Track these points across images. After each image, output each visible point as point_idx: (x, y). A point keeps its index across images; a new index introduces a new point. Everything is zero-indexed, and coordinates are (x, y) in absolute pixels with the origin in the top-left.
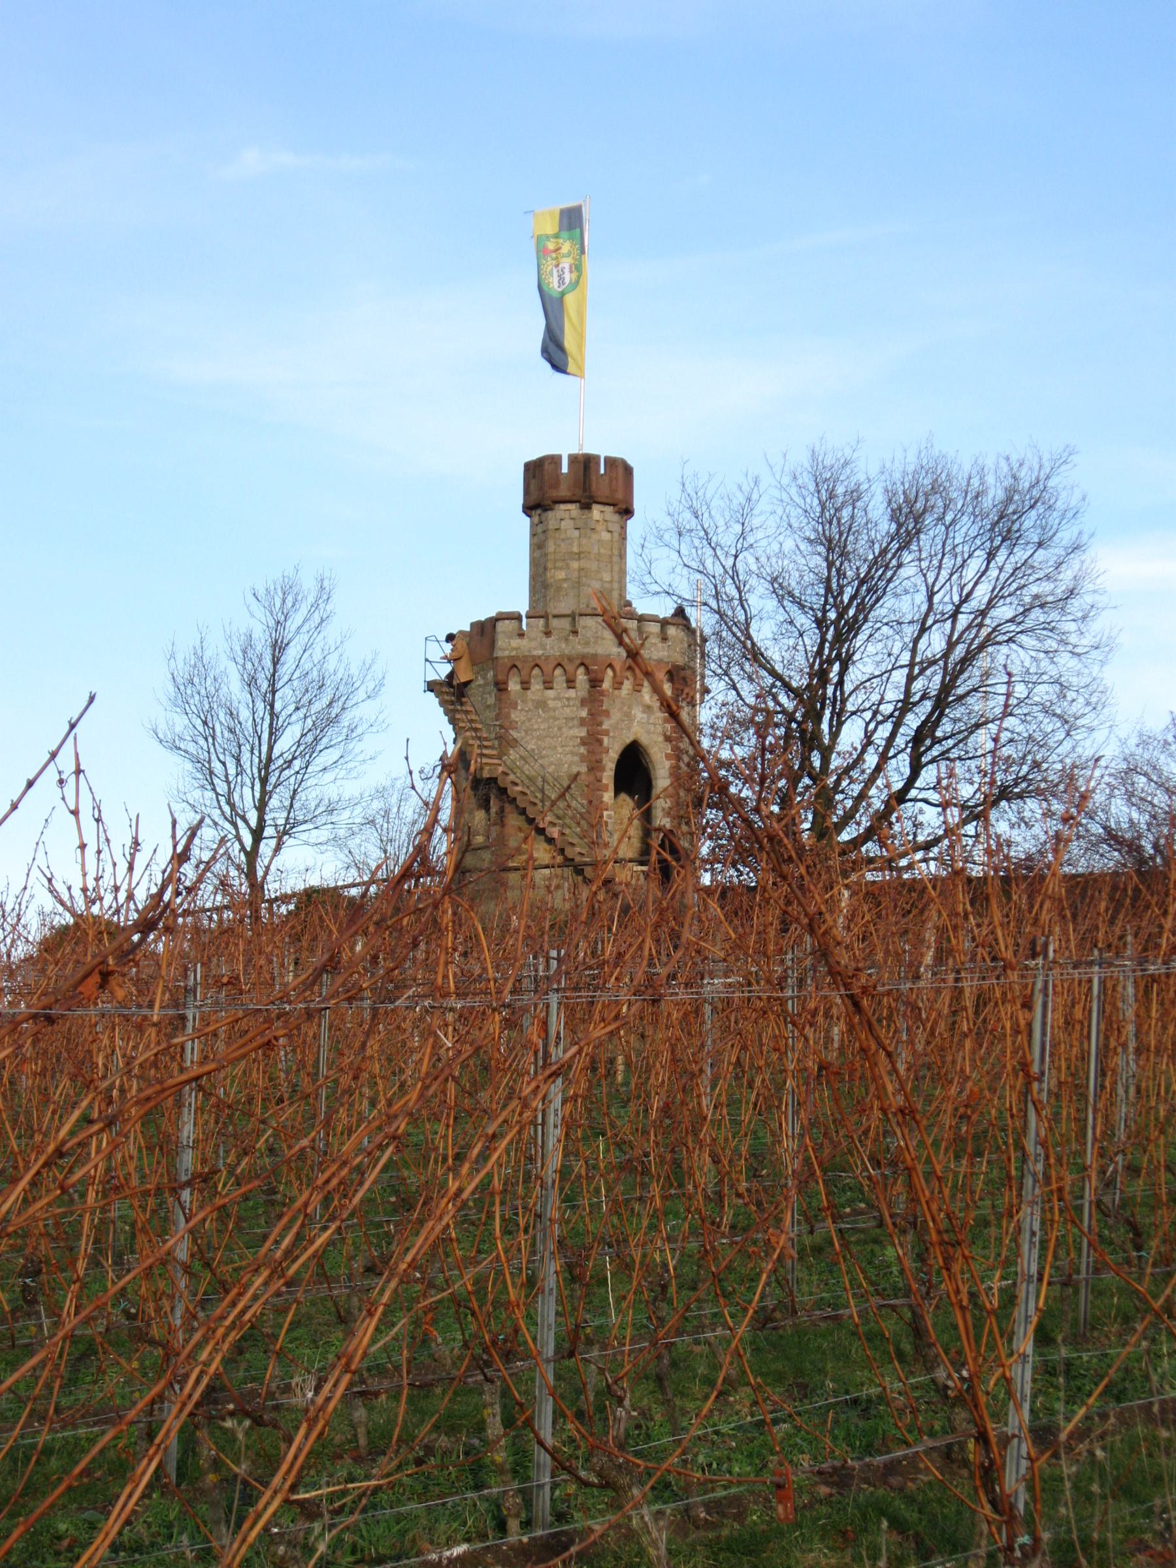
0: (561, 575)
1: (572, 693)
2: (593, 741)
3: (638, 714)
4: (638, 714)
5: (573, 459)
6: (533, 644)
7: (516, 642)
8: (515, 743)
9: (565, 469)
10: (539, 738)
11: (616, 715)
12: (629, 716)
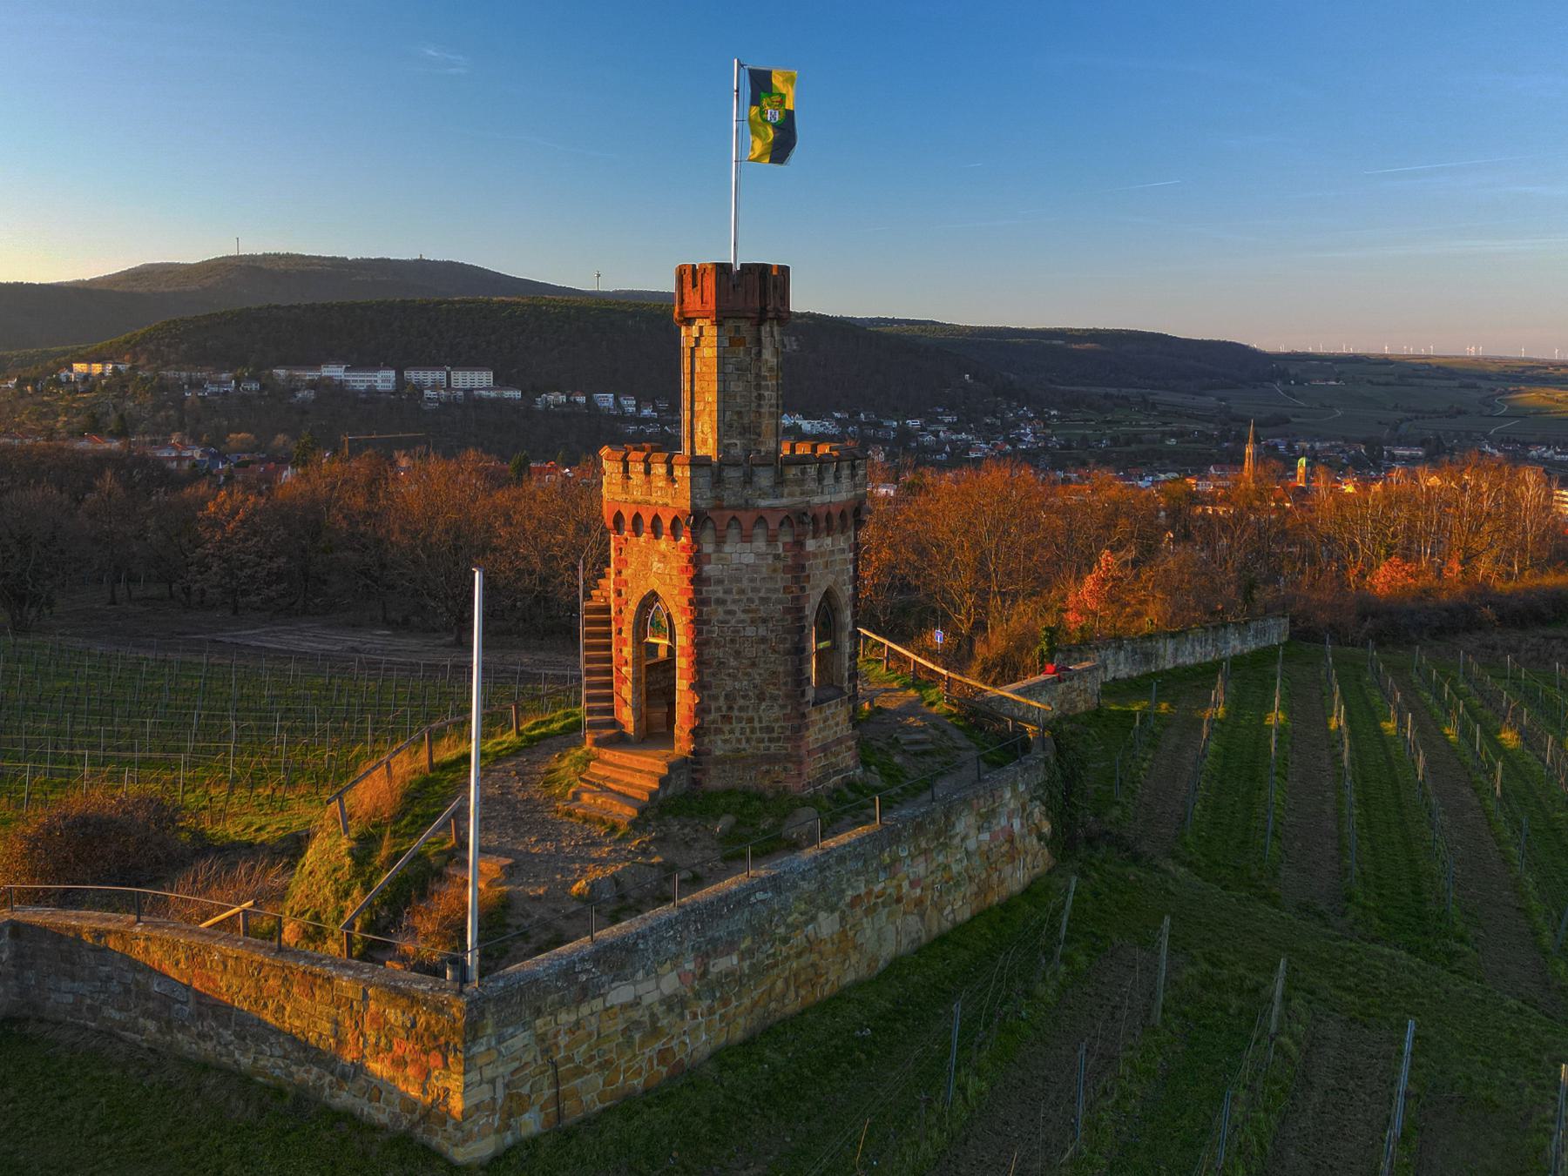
4: (657, 566)
12: (646, 566)
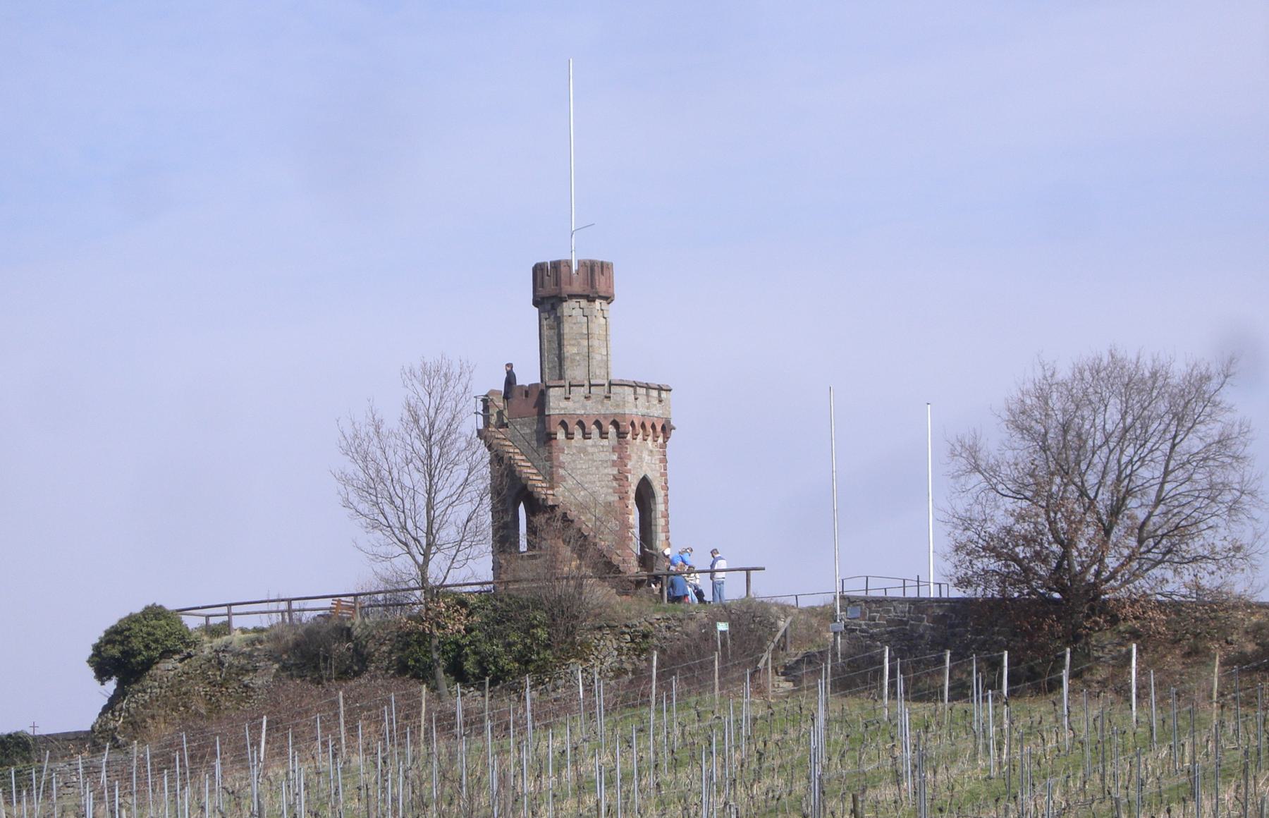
0: (575, 350)
1: (605, 442)
2: (621, 478)
3: (646, 456)
4: (646, 456)
5: (582, 264)
6: (577, 405)
7: (564, 404)
8: (563, 478)
9: (575, 267)
10: (582, 475)
11: (634, 457)
12: (640, 458)
